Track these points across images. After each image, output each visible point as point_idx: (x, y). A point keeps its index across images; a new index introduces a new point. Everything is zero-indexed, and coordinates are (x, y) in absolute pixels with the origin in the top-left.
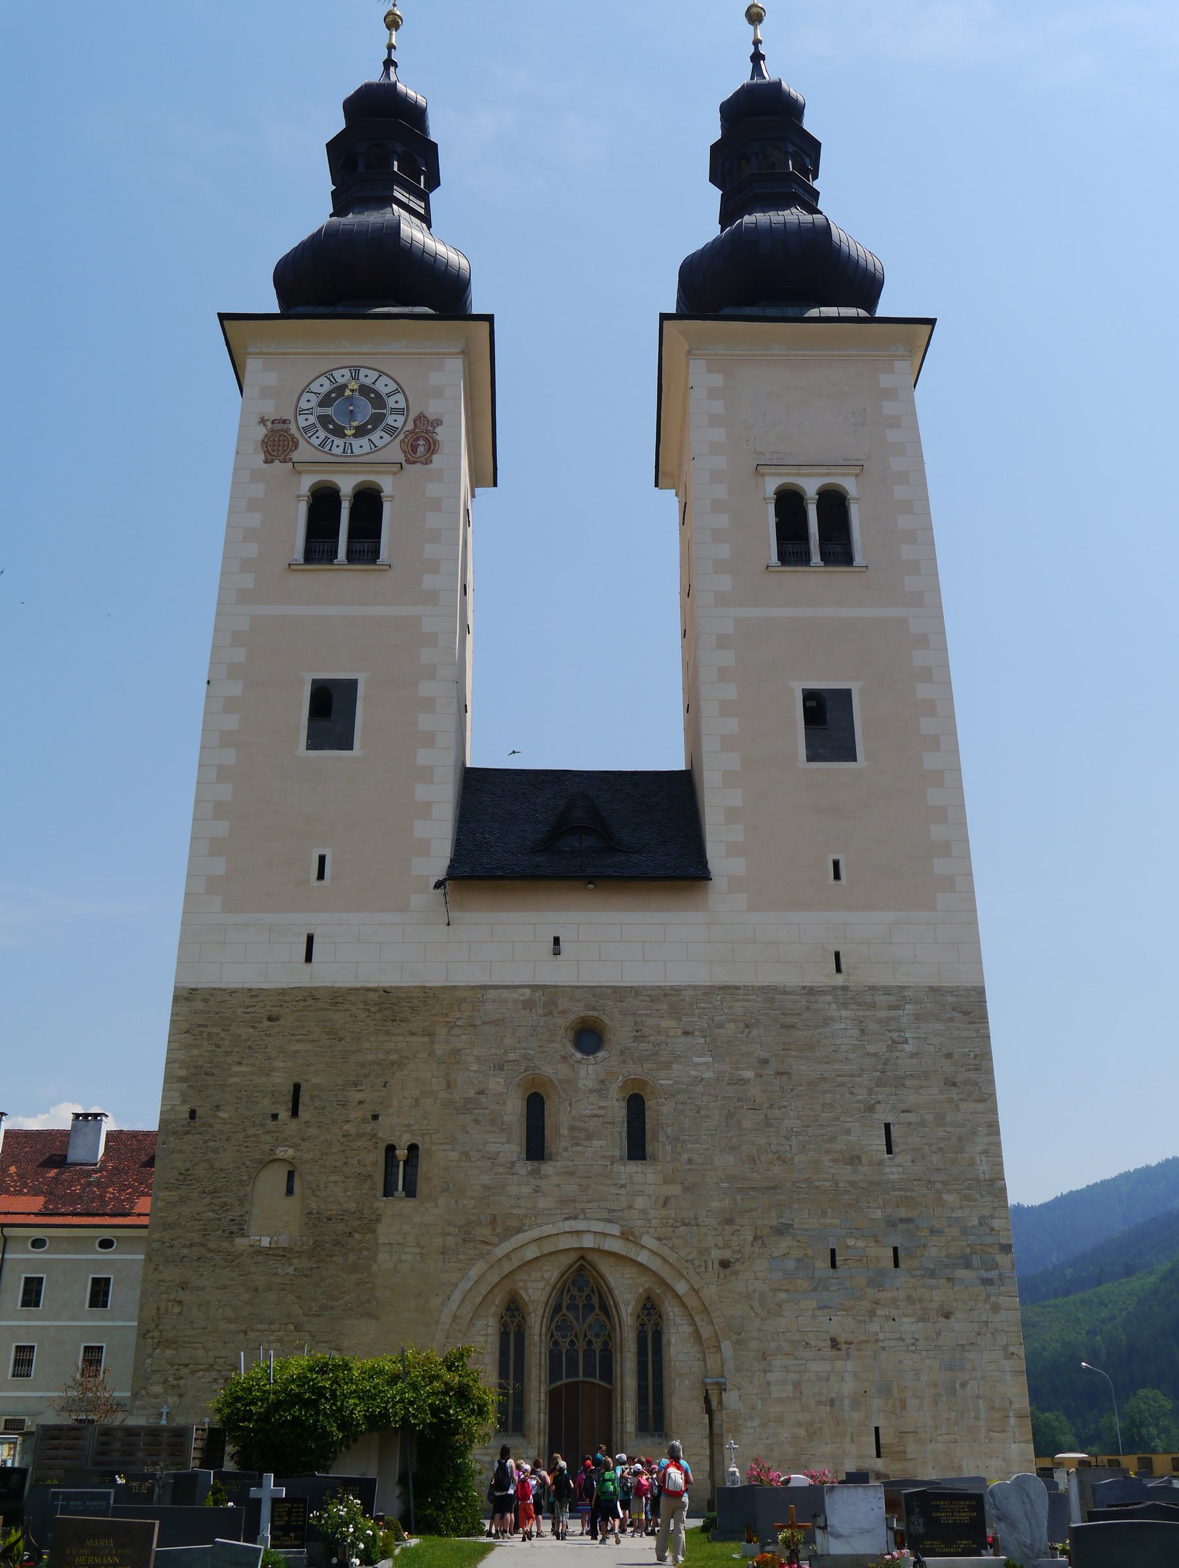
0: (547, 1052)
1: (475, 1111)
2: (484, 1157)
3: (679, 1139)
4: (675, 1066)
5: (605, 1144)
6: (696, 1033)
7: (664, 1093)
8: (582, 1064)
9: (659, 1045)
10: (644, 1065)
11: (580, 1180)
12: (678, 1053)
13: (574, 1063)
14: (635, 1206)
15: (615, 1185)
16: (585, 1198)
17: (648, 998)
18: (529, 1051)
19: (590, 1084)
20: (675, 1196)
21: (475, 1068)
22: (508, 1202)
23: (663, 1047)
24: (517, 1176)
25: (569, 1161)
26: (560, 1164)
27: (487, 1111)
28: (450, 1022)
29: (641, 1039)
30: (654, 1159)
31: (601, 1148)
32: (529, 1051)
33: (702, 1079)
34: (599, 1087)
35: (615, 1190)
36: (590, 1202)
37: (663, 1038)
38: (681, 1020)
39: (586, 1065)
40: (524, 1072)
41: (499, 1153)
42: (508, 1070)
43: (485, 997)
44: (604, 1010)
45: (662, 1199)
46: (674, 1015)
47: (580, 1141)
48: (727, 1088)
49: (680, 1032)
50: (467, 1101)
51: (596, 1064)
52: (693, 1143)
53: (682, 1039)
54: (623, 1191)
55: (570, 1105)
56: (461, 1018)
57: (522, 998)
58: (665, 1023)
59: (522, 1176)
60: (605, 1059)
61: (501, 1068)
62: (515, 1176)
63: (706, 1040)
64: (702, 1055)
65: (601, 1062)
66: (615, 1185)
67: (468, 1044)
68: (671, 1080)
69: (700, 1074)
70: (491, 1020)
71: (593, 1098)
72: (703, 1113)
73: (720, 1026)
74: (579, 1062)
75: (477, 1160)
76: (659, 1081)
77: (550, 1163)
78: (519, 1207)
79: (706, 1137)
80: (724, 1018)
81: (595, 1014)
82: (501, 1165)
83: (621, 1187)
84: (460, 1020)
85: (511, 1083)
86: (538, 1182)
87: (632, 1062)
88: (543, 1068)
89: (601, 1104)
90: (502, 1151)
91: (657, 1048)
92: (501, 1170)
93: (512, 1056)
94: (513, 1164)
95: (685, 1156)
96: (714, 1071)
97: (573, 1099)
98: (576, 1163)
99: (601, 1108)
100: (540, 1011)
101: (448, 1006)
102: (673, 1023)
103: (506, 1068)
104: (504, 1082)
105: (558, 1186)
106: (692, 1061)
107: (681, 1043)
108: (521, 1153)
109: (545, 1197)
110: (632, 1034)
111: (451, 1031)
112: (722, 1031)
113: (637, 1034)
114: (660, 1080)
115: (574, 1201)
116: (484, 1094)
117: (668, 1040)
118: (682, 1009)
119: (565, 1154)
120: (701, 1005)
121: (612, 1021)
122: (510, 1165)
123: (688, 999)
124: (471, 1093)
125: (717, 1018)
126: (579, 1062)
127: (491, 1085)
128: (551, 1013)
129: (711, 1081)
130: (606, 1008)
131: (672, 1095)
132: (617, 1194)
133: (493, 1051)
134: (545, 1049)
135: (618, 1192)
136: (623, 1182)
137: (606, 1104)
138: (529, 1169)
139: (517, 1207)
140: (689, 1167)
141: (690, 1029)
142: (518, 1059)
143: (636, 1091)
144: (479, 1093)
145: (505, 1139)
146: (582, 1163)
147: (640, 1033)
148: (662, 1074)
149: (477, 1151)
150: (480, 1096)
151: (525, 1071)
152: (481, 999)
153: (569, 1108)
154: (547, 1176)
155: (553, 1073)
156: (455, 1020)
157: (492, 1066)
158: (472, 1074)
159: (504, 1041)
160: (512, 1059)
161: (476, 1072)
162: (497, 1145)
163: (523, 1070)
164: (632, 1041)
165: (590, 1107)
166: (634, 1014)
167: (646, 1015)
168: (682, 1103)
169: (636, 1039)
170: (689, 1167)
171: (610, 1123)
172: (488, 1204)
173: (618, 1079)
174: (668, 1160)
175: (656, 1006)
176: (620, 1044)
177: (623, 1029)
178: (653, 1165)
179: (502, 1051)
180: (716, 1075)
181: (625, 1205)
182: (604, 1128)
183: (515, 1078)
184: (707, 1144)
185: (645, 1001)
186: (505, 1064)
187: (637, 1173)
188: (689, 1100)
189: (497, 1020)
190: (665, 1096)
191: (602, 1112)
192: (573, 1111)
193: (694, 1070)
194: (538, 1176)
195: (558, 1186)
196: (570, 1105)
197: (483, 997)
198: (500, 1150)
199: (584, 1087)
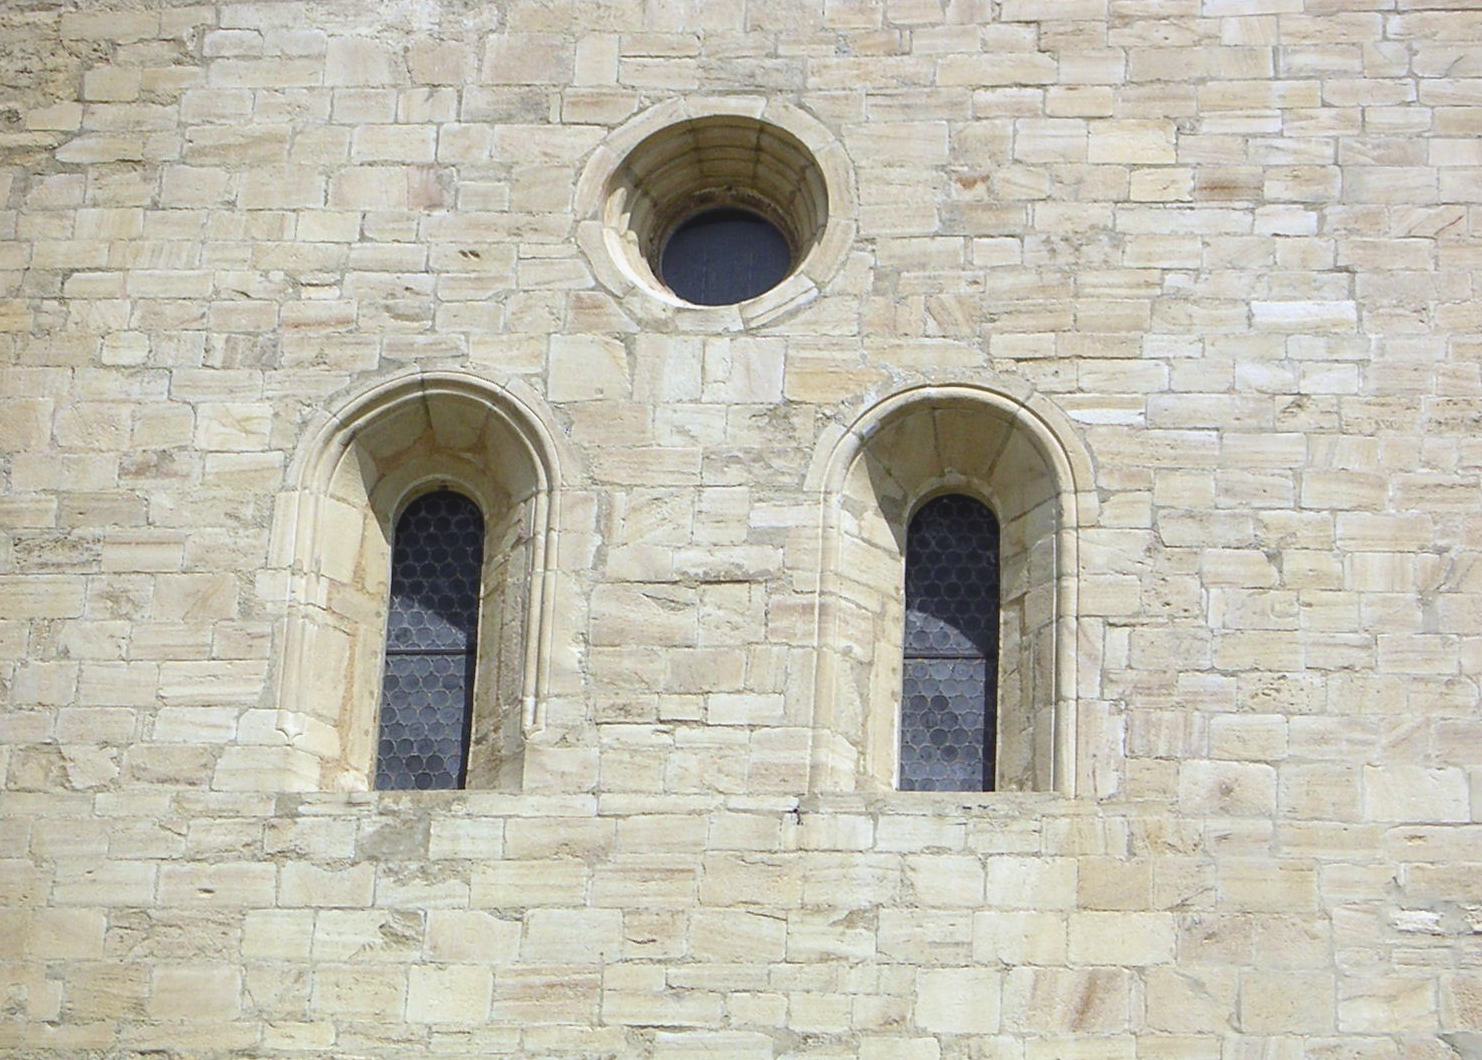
0: (502, 279)
1: (113, 556)
2: (136, 773)
3: (1167, 687)
4: (1153, 344)
5: (767, 706)
6: (1271, 190)
7: (1097, 468)
8: (677, 332)
9: (1074, 243)
10: (995, 338)
11: (634, 887)
12: (1171, 279)
13: (634, 328)
14: (921, 1023)
15: (817, 910)
16: (656, 977)
17: (1028, 34)
18: (407, 279)
19: (715, 429)
20: (1141, 970)
21: (136, 356)
22: (245, 991)
23: (1093, 253)
24: (303, 863)
25: (580, 790)
26: (527, 805)
27: (174, 556)
28: (27, 150)
29: (987, 219)
30: (1039, 775)
31: (752, 727)
32: (407, 279)
33: (1300, 401)
34: (754, 441)
35: (813, 936)
36: (678, 996)
37: (1100, 214)
38: (1193, 131)
39: (697, 341)
40: (380, 371)
41: (217, 752)
42: (299, 364)
43: (209, 38)
44: (802, 90)
45: (1068, 986)
46: (1158, 109)
47: (644, 698)
48: (1431, 442)
49: (1185, 183)
50: (75, 507)
51: (748, 331)
52: (1241, 709)
53: (1207, 216)
54: (860, 944)
55: (605, 522)
56: (80, 134)
57: (394, 42)
58: (1113, 144)
59: (333, 864)
60: (793, 314)
61: (266, 360)
62: (291, 867)
63: (1322, 219)
64: (1307, 288)
65: (775, 322)
66: (817, 910)
67: (104, 247)
68: (1133, 404)
69: (1289, 376)
70: (231, 140)
71: (728, 495)
72: (1294, 561)
73: (1402, 153)
74: (660, 326)
75: (102, 788)
76: (1074, 414)
77: (477, 799)
78: (306, 1019)
79: (1317, 679)
80: (1420, 116)
81: (756, 108)
82: (219, 814)
83: (852, 919)
84: (77, 142)
85: (305, 423)
86: (413, 894)
87: (932, 326)
88: (477, 354)
89: (764, 516)
90: (234, 742)
91: (1065, 258)
92: (218, 836)
93: (323, 302)
94: (288, 807)
95: (1200, 774)
96: (1362, 363)
97: (620, 496)
98: (614, 802)
99: (760, 537)
100: (477, 100)
101: (24, 80)
102: (1153, 144)
103: (288, 356)
104: (276, 415)
105: (518, 914)
106: (1250, 317)
107: (1192, 235)
108: (342, 763)
109: (441, 967)
110: (940, 197)
111: (25, 190)
112: (1413, 176)
113: (968, 196)
114: (1078, 405)
115: (592, 989)
116: (167, 475)
117: (1126, 221)
118: (1202, 81)
119: (564, 760)
120: (1300, 60)
121: (840, 139)
122: (270, 809)
123: (1231, 33)
124: (100, 475)
125: (1383, 116)
126: (660, 326)
127: (208, 432)
128: (533, 108)
129: (1348, 412)
130: (812, 81)
131: (1138, 479)
132: (825, 957)
133: (231, 279)
134: (492, 268)
135: (830, 944)
136: (862, 898)
137: (788, 516)
138: (369, 828)
139: (290, 1016)
140: (1223, 824)
141: (1243, 172)
142: (352, 310)
143: (954, 479)
144: (141, 471)
145: (259, 688)
146: (651, 802)
147: (980, 188)
148: (1088, 375)
149: (105, 744)
150: (143, 483)
151: (387, 364)
152: (190, 46)
153: (598, 540)
154: (454, 866)
155: (527, 377)
156: (49, 140)
157: (219, 341)
158: (112, 383)
159: (288, 234)
160: (324, 315)
161: (133, 371)
162: (216, 715)
163: (376, 367)
164: (936, 226)
165: (705, 534)
166: (955, 105)
167: (1018, 112)
168: (1190, 515)
169: (952, 222)
170: (1223, 824)
171: (807, 609)
172: (139, 1006)
173: (860, 399)
174: (1108, 785)
175: (1069, 71)
176: (872, 241)
177: (894, 173)
178: (1024, 813)
179: (278, 276)
180: (1372, 385)
181: (868, 1011)
182: (774, 631)
183: (331, 399)
184: (1322, 712)
185: (1012, 48)
186: (288, 335)
187: (939, 851)
188: (1224, 501)
189: (259, 140)
190: (1103, 482)
191: (766, 558)
192: (615, 555)
193: (1263, 359)
194: (414, 866)
195: (518, 914)
196: (605, 522)
197: (200, 32)
198: (220, 737)
199: (677, 439)
